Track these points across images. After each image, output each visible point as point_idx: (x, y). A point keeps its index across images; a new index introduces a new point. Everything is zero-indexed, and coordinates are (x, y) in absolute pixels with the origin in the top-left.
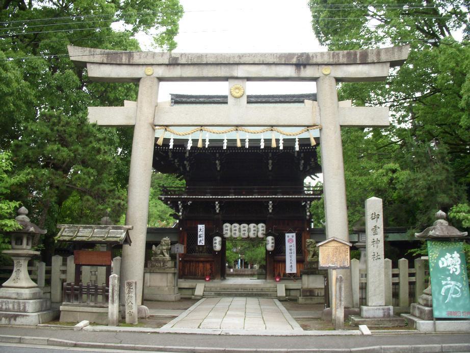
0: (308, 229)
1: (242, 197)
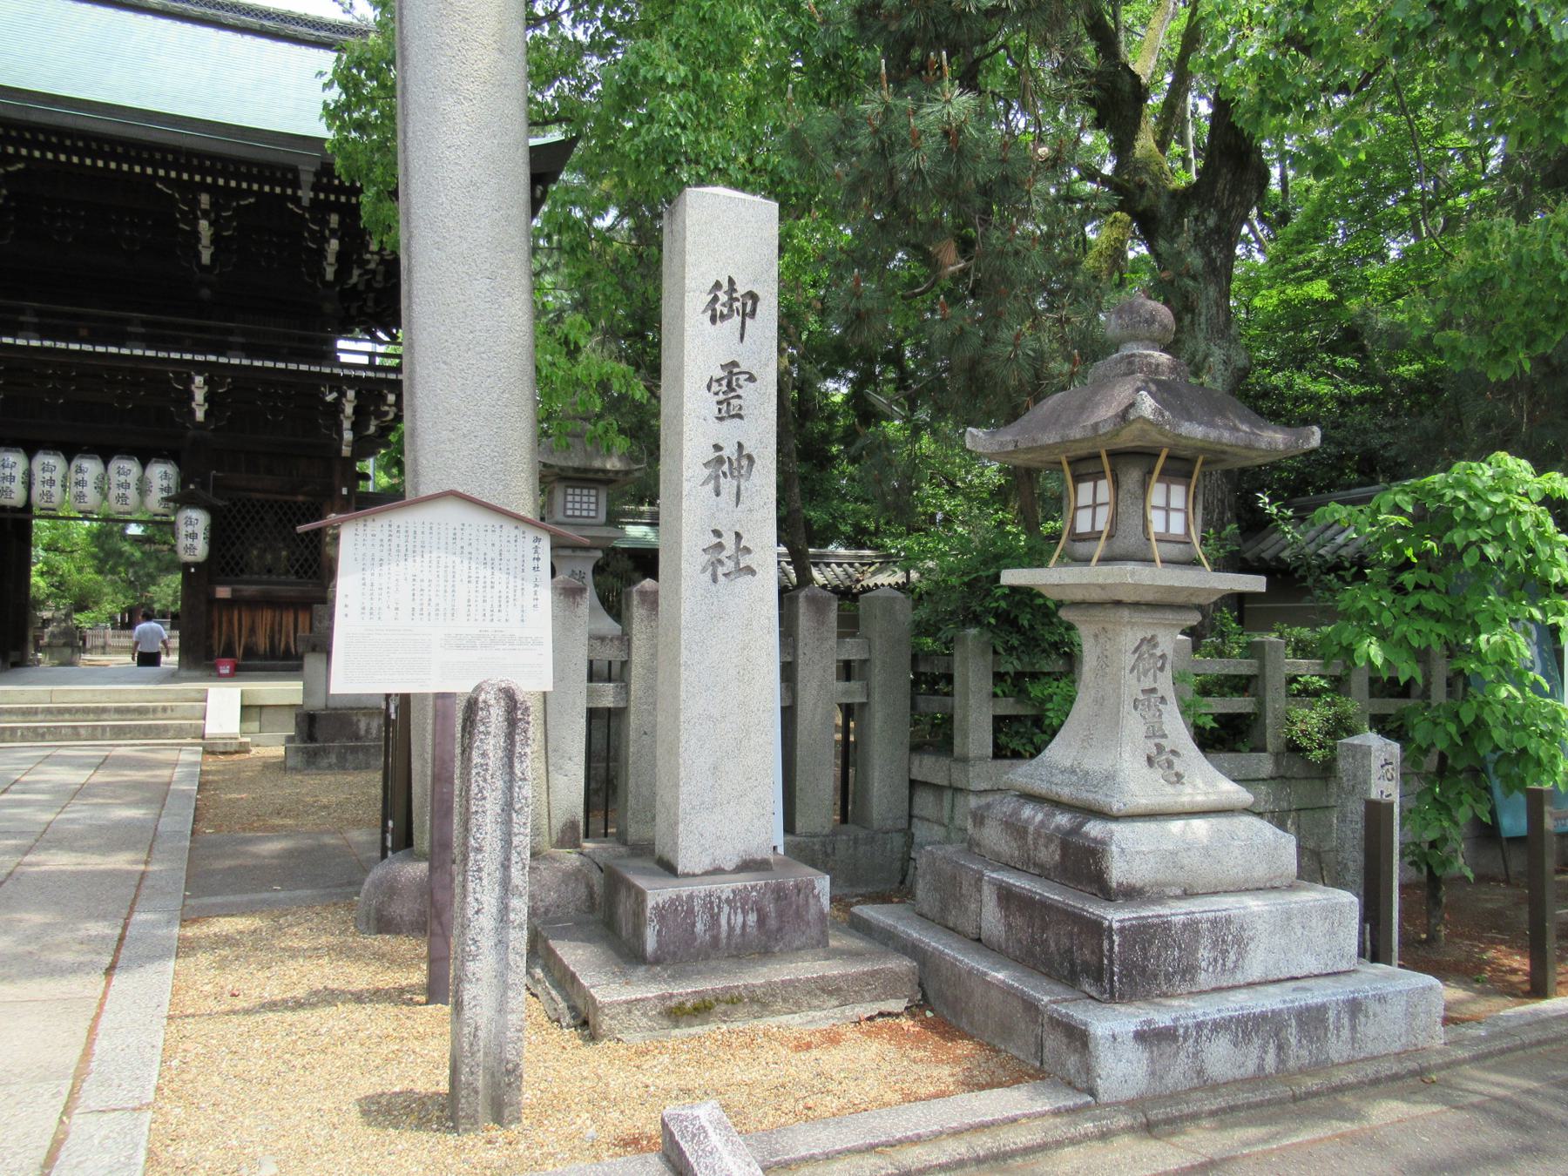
0: (345, 491)
1: (75, 347)
